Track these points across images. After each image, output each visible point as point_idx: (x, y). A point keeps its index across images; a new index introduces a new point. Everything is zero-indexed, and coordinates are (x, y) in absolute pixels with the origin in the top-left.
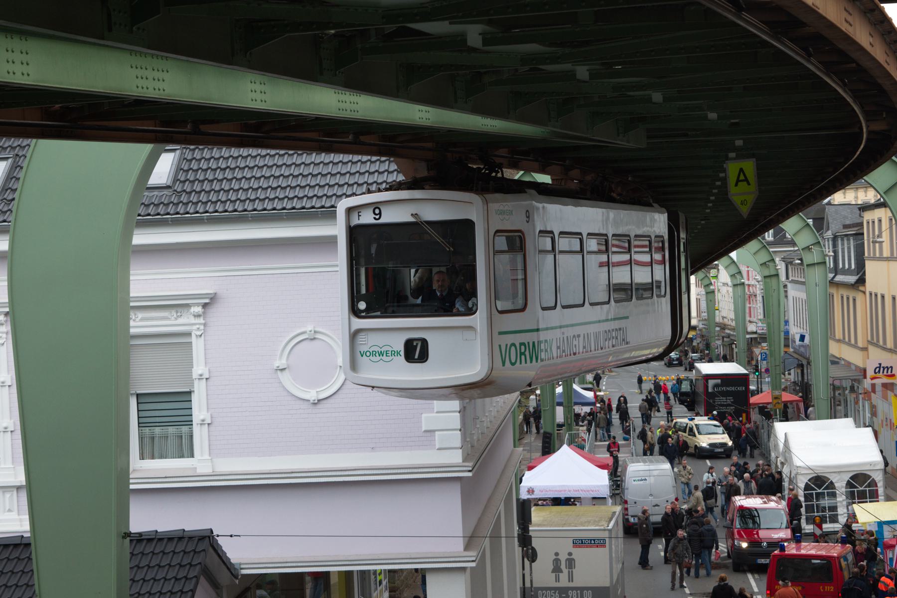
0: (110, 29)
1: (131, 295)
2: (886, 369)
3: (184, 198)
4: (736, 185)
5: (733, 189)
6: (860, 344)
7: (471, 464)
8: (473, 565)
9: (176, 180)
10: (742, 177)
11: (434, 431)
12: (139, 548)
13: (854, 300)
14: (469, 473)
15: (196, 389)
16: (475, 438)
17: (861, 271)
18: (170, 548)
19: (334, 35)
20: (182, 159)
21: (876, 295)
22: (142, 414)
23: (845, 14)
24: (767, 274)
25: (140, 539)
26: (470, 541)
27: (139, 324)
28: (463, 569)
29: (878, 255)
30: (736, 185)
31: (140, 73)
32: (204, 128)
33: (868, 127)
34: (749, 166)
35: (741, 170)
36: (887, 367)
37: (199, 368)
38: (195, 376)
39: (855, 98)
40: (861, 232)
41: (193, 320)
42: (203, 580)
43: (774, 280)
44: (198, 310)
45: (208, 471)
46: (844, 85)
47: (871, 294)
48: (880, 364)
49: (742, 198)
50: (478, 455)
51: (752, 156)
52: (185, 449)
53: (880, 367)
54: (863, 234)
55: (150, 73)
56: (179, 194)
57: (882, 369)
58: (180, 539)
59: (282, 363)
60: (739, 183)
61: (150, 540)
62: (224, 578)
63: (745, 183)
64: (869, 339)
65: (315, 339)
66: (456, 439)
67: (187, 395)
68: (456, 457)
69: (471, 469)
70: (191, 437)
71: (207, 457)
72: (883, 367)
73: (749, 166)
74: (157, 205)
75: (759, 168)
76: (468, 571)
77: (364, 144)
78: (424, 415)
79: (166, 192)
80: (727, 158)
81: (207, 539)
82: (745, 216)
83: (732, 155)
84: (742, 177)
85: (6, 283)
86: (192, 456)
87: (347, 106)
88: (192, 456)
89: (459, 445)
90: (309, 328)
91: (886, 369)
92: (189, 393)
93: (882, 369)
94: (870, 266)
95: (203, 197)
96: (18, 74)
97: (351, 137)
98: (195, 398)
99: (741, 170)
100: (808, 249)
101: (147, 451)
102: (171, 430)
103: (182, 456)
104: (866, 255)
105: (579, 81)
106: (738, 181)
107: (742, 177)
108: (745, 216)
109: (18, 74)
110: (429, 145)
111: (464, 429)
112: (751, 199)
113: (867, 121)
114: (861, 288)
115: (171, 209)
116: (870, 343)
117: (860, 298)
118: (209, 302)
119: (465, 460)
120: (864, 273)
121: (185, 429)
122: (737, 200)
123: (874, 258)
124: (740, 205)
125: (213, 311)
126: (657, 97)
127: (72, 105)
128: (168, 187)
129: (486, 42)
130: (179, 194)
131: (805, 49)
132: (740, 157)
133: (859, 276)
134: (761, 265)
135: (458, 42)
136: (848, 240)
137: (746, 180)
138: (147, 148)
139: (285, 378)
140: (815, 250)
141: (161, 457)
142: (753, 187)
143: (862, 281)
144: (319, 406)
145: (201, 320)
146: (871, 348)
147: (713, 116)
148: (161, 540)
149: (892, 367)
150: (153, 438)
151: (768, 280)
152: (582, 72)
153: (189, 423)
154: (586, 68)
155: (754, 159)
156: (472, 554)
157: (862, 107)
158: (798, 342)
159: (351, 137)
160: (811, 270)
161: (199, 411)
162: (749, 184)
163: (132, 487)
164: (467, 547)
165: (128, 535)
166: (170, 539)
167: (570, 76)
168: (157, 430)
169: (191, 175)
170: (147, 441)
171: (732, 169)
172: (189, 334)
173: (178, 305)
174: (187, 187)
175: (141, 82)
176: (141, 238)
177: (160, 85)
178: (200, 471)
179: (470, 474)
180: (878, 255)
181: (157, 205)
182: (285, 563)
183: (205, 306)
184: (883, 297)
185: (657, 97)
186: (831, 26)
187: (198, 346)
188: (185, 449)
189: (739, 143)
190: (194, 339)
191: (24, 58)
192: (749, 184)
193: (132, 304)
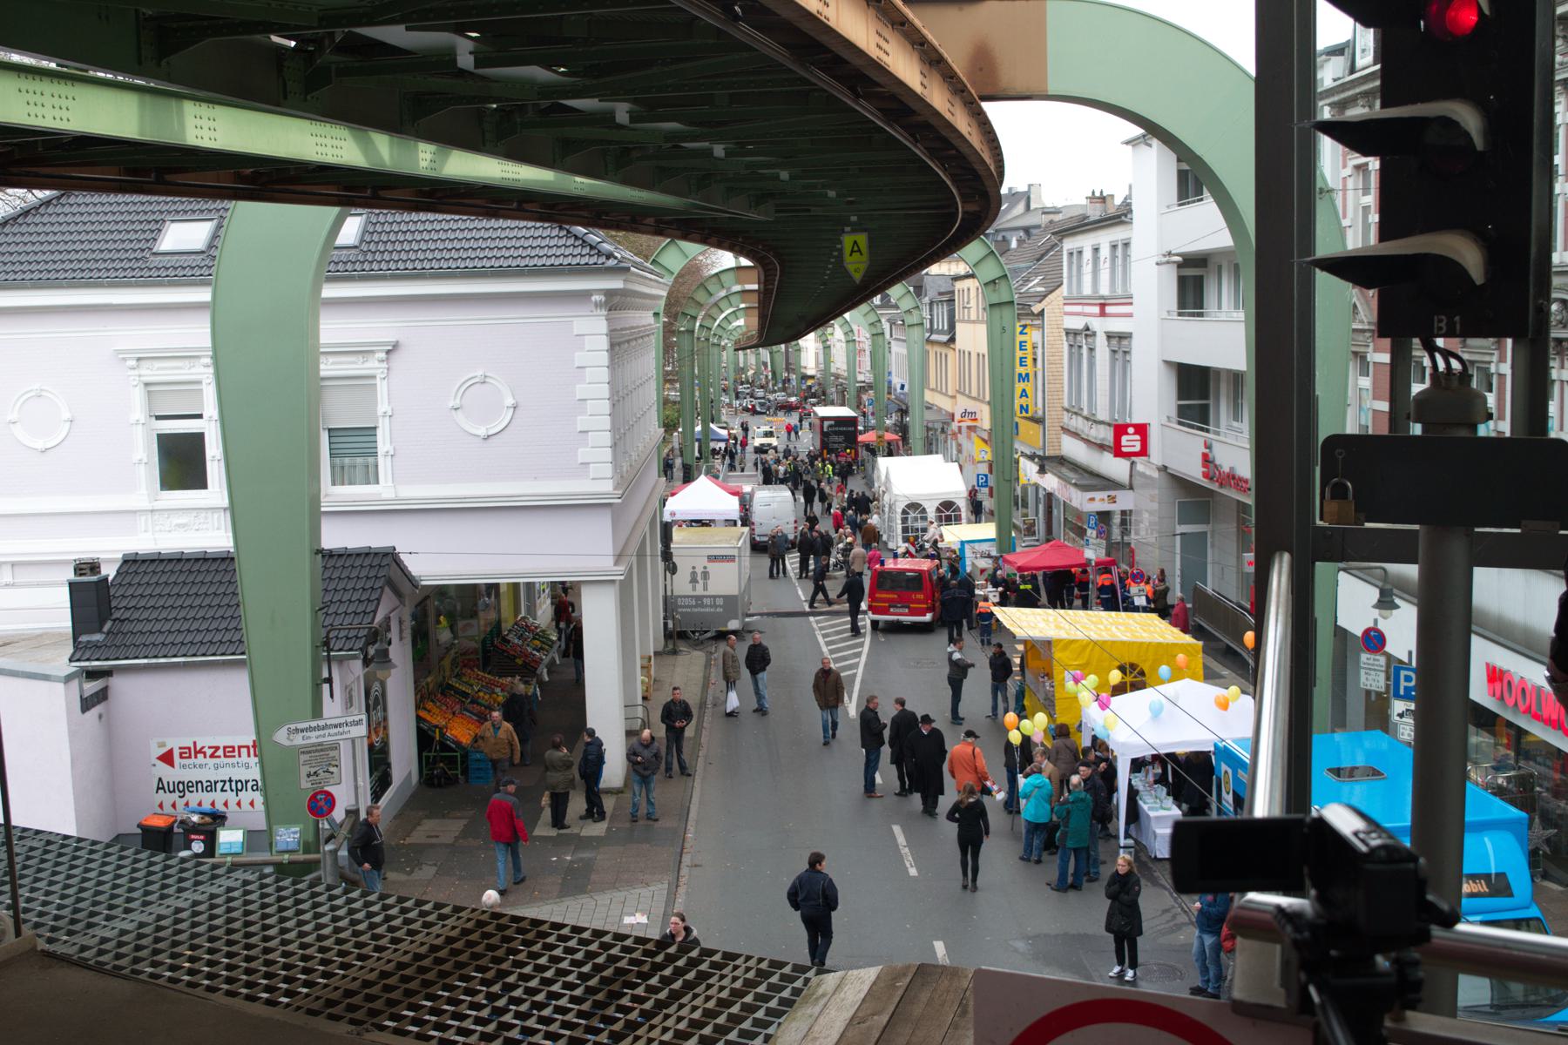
0: (285, 97)
1: (321, 341)
3: (369, 256)
5: (848, 259)
6: (950, 393)
7: (620, 492)
8: (622, 578)
9: (362, 241)
10: (856, 249)
11: (589, 463)
12: (332, 562)
13: (946, 356)
15: (380, 425)
16: (625, 469)
18: (358, 563)
19: (495, 109)
20: (368, 222)
22: (333, 446)
23: (949, 105)
25: (330, 555)
26: (618, 558)
27: (327, 367)
28: (613, 581)
29: (966, 318)
31: (319, 140)
32: (382, 193)
33: (963, 207)
34: (862, 239)
35: (855, 242)
37: (383, 407)
38: (380, 413)
39: (954, 181)
41: (377, 364)
42: (387, 589)
43: (880, 338)
44: (383, 355)
45: (393, 496)
46: (945, 170)
49: (857, 266)
50: (627, 484)
51: (865, 230)
52: (371, 476)
54: (954, 300)
55: (328, 141)
56: (365, 253)
58: (367, 554)
59: (457, 403)
61: (340, 556)
62: (406, 588)
65: (484, 382)
66: (608, 470)
67: (372, 431)
68: (607, 486)
70: (377, 466)
71: (390, 484)
73: (862, 239)
74: (345, 263)
76: (618, 583)
77: (527, 211)
78: (580, 450)
79: (353, 251)
80: (843, 232)
81: (389, 557)
82: (858, 282)
83: (848, 229)
84: (856, 249)
85: (209, 330)
86: (378, 483)
87: (510, 176)
88: (378, 483)
89: (610, 475)
90: (480, 373)
92: (375, 428)
94: (958, 326)
95: (387, 256)
96: (206, 139)
97: (515, 205)
98: (379, 432)
99: (855, 242)
100: (909, 311)
101: (338, 479)
102: (359, 460)
103: (368, 483)
104: (957, 317)
105: (715, 158)
106: (852, 251)
107: (856, 249)
108: (858, 282)
109: (206, 139)
110: (585, 214)
111: (615, 462)
112: (863, 267)
113: (963, 202)
114: (952, 346)
115: (358, 266)
116: (958, 392)
117: (950, 353)
118: (393, 349)
119: (615, 489)
120: (954, 334)
121: (371, 460)
122: (851, 268)
123: (963, 321)
125: (395, 357)
126: (784, 175)
127: (262, 170)
128: (356, 247)
129: (632, 120)
130: (365, 253)
131: (912, 135)
132: (854, 231)
135: (607, 119)
137: (859, 251)
138: (335, 210)
139: (459, 416)
140: (915, 312)
141: (350, 484)
142: (865, 258)
143: (952, 340)
144: (490, 441)
145: (385, 365)
146: (958, 395)
147: (832, 194)
148: (350, 555)
150: (343, 467)
151: (875, 337)
152: (719, 150)
153: (375, 455)
154: (722, 146)
156: (622, 568)
157: (958, 189)
158: (899, 390)
159: (515, 205)
160: (911, 329)
161: (383, 444)
163: (323, 509)
164: (616, 563)
165: (320, 551)
166: (358, 555)
167: (708, 153)
168: (347, 461)
169: (376, 237)
170: (338, 469)
171: (848, 241)
172: (374, 377)
173: (364, 352)
174: (373, 247)
175: (319, 149)
176: (330, 291)
177: (338, 152)
178: (384, 496)
179: (619, 501)
180: (966, 318)
181: (345, 263)
182: (460, 576)
183: (388, 352)
184: (970, 354)
185: (784, 175)
186: (937, 114)
187: (382, 387)
188: (371, 476)
189: (854, 219)
190: (378, 381)
191: (211, 124)
193: (322, 350)
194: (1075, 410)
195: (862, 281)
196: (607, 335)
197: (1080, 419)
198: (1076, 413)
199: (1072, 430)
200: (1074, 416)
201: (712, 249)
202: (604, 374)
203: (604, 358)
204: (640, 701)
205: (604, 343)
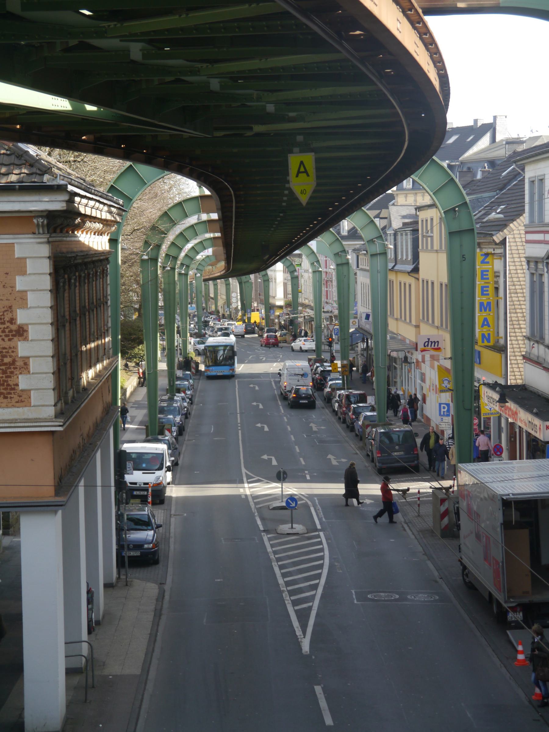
2: (433, 343)
4: (297, 176)
6: (414, 322)
10: (302, 169)
14: (61, 427)
17: (415, 262)
21: (427, 282)
24: (339, 262)
29: (429, 248)
30: (297, 176)
34: (309, 159)
35: (302, 163)
36: (434, 342)
40: (416, 228)
43: (345, 267)
47: (423, 281)
48: (429, 339)
53: (428, 342)
54: (418, 230)
57: (430, 343)
60: (300, 175)
63: (305, 174)
64: (421, 318)
66: (50, 398)
69: (62, 424)
72: (432, 342)
73: (309, 159)
75: (317, 160)
80: (291, 152)
84: (302, 169)
91: (433, 343)
93: (430, 343)
94: (423, 256)
99: (302, 163)
106: (299, 172)
107: (302, 170)
114: (416, 275)
120: (418, 263)
122: (297, 190)
124: (300, 195)
132: (301, 151)
133: (414, 265)
134: (335, 254)
136: (406, 235)
137: (306, 172)
143: (416, 270)
149: (438, 342)
151: (340, 268)
155: (313, 154)
162: (308, 175)
180: (429, 248)
184: (433, 283)
192: (308, 175)
194: (538, 339)
195: (308, 203)
196: (49, 257)
197: (542, 347)
198: (538, 342)
199: (536, 359)
200: (536, 345)
201: (166, 172)
202: (47, 299)
203: (47, 282)
204: (84, 635)
205: (46, 266)
